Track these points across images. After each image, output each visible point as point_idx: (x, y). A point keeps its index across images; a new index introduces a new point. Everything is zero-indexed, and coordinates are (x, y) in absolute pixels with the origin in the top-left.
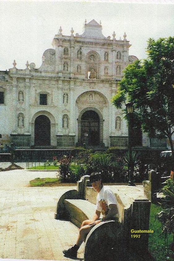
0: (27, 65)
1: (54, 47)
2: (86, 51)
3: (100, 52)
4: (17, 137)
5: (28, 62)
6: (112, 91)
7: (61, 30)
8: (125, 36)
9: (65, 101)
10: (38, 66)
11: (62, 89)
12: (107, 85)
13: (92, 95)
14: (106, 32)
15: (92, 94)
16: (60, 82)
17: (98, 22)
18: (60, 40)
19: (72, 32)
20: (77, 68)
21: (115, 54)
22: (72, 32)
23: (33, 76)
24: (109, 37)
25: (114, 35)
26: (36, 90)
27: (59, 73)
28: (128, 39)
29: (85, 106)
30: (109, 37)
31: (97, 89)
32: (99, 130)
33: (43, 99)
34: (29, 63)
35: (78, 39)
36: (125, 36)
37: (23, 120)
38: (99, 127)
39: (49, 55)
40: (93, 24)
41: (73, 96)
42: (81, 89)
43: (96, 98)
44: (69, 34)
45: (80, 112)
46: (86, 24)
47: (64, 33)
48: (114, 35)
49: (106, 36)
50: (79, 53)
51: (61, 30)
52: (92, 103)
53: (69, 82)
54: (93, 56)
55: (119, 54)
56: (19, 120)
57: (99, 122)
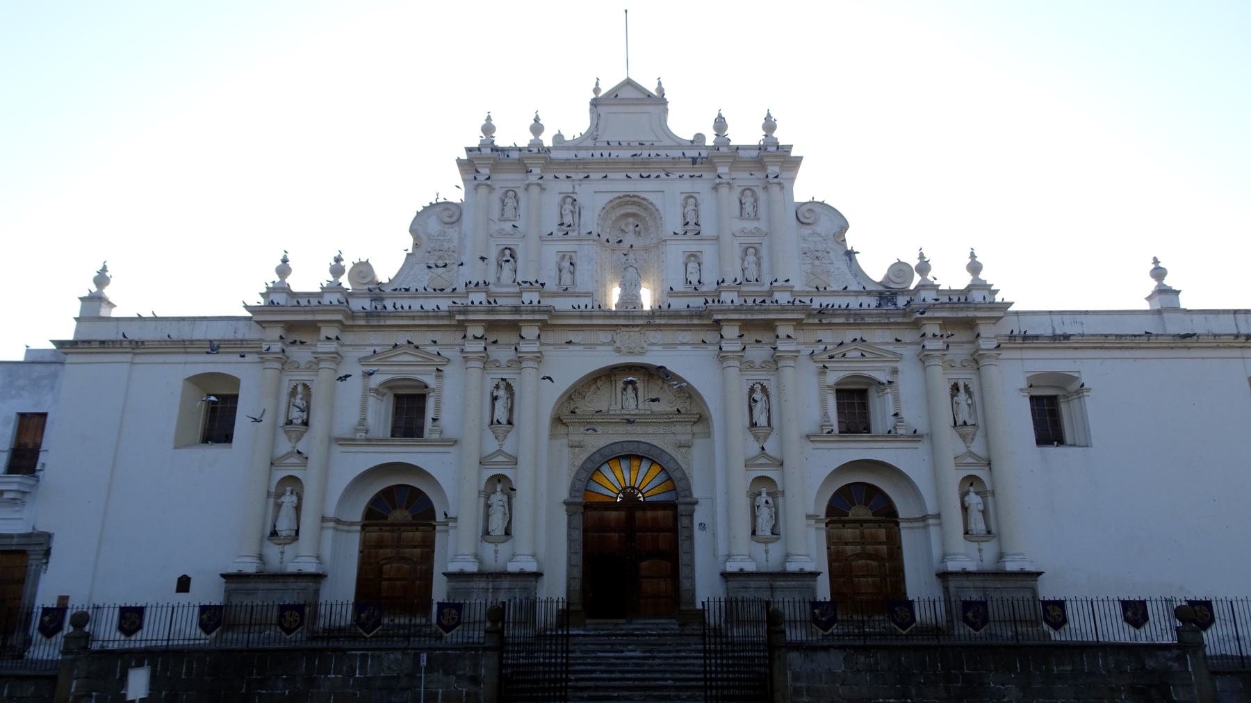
0: (337, 270)
1: (453, 190)
3: (667, 197)
4: (251, 585)
6: (722, 357)
7: (488, 129)
8: (769, 125)
10: (385, 271)
13: (635, 389)
14: (688, 121)
17: (652, 89)
18: (484, 163)
19: (537, 128)
20: (560, 271)
21: (730, 199)
22: (537, 128)
23: (353, 315)
24: (700, 137)
30: (700, 137)
31: (654, 358)
33: (410, 411)
34: (348, 265)
36: (769, 125)
37: (298, 508)
38: (674, 530)
39: (434, 224)
40: (628, 93)
44: (523, 139)
45: (579, 462)
46: (594, 100)
47: (502, 140)
49: (687, 135)
51: (488, 129)
55: (748, 201)
56: (278, 506)
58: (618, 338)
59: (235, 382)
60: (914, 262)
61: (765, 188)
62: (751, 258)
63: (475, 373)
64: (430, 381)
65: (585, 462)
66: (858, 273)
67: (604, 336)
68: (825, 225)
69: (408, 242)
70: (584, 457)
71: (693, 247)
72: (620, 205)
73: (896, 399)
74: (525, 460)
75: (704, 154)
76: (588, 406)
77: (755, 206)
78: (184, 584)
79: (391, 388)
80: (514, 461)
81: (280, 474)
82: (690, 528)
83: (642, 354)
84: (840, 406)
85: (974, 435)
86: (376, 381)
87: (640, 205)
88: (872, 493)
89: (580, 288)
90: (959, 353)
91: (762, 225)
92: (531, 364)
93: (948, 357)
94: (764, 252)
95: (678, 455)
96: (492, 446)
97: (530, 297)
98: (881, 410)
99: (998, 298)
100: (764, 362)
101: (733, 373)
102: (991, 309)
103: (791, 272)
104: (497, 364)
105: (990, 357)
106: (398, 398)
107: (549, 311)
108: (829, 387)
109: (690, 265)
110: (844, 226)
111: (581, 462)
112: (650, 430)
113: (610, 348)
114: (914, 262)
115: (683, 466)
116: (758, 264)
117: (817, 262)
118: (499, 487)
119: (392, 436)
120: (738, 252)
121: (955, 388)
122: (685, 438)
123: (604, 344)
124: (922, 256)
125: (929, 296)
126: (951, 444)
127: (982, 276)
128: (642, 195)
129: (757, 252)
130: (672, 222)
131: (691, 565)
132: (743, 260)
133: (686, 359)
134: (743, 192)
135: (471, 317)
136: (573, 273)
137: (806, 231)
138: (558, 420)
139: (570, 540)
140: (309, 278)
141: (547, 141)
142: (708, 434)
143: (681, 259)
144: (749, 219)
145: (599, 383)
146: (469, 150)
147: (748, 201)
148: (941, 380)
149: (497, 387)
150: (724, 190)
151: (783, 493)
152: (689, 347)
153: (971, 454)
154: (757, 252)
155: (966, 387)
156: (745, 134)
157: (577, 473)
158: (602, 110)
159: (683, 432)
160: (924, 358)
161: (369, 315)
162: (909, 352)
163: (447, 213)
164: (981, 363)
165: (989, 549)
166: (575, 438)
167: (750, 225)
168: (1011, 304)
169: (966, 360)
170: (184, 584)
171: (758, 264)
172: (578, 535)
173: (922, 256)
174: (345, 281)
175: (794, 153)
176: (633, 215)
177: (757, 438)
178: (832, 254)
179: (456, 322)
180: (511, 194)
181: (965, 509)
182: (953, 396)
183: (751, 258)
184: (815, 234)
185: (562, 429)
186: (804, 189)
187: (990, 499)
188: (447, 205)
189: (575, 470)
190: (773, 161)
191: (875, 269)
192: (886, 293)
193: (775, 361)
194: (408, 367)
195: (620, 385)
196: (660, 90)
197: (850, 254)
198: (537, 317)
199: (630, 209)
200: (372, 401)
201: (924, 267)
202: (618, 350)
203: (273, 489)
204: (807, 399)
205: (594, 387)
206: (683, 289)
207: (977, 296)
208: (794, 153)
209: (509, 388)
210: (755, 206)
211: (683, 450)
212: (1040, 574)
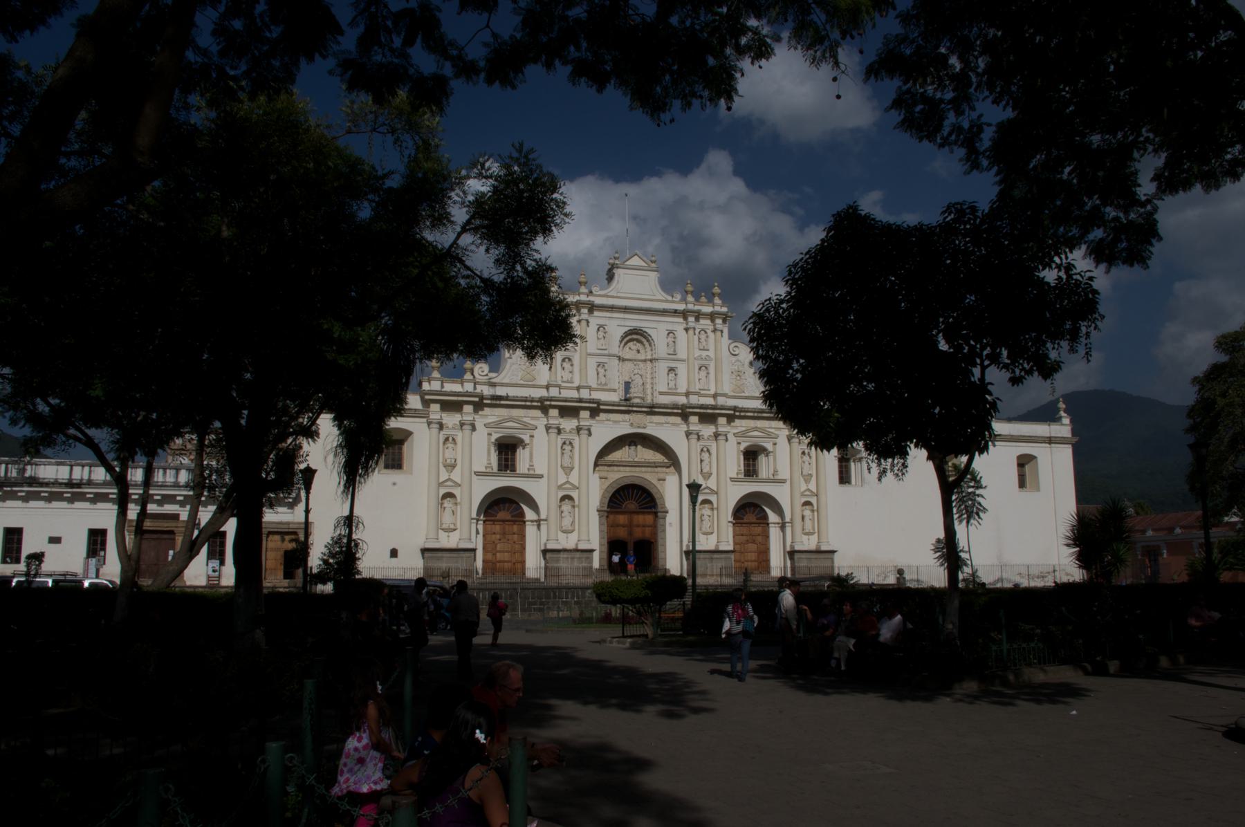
3: (657, 328)
4: (440, 554)
12: (678, 420)
23: (482, 397)
26: (490, 434)
29: (617, 476)
31: (651, 430)
32: (655, 534)
38: (654, 526)
42: (607, 429)
45: (605, 487)
50: (601, 334)
55: (703, 336)
57: (656, 514)
59: (408, 434)
64: (526, 438)
70: (608, 483)
71: (673, 365)
73: (775, 460)
76: (617, 456)
78: (394, 553)
81: (443, 491)
82: (664, 525)
88: (756, 506)
96: (562, 479)
122: (661, 476)
130: (661, 348)
131: (664, 545)
133: (670, 432)
137: (734, 359)
138: (596, 465)
139: (601, 531)
150: (691, 332)
165: (814, 539)
166: (604, 474)
167: (704, 353)
170: (394, 553)
172: (605, 528)
179: (543, 406)
181: (803, 517)
194: (510, 429)
202: (632, 425)
212: (833, 552)
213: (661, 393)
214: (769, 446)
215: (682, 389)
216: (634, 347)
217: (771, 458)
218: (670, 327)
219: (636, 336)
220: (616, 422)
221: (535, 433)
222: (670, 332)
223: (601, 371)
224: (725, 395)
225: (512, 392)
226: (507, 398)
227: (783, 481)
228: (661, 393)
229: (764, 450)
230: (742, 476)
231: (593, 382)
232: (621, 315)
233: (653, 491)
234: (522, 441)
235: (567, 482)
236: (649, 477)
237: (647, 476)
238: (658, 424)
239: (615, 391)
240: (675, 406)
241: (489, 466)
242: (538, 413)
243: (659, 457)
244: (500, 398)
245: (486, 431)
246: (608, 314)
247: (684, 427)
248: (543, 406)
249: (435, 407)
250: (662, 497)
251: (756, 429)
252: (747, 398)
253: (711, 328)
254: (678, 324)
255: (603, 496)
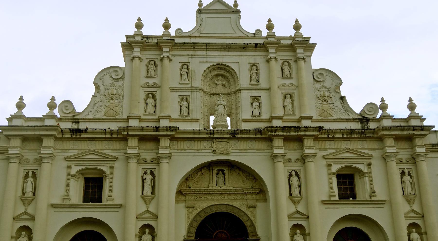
0: (52, 106)
1: (118, 60)
2: (200, 64)
3: (241, 64)
5: (53, 99)
6: (274, 157)
7: (139, 25)
8: (297, 27)
9: (148, 190)
10: (80, 107)
11: (140, 161)
15: (223, 171)
16: (133, 142)
19: (167, 26)
20: (181, 107)
21: (276, 67)
22: (167, 26)
23: (62, 131)
25: (270, 26)
27: (130, 121)
28: (305, 32)
31: (235, 156)
33: (94, 188)
34: (58, 102)
35: (177, 41)
36: (297, 27)
39: (107, 79)
41: (172, 175)
43: (233, 182)
44: (159, 31)
45: (192, 217)
48: (270, 26)
49: (251, 30)
50: (185, 70)
52: (225, 195)
53: (156, 140)
54: (222, 75)
55: (286, 68)
58: (214, 145)
60: (378, 103)
61: (296, 61)
62: (288, 100)
63: (133, 166)
64: (106, 170)
65: (195, 217)
66: (348, 109)
67: (206, 144)
68: (329, 80)
69: (92, 91)
70: (194, 213)
71: (256, 94)
72: (214, 70)
73: (371, 181)
74: (163, 216)
75: (261, 41)
77: (290, 72)
79: (82, 174)
80: (156, 217)
83: (227, 154)
84: (339, 184)
85: (414, 200)
86: (74, 170)
87: (225, 70)
89: (193, 116)
90: (404, 154)
91: (294, 82)
92: (165, 160)
93: (399, 157)
94: (295, 97)
95: (248, 212)
97: (164, 123)
98: (362, 188)
99: (425, 123)
100: (297, 159)
101: (280, 165)
102: (422, 130)
103: (310, 109)
104: (145, 161)
105: (422, 156)
106: (87, 180)
107: (175, 129)
108: (333, 173)
109: (254, 104)
110: (341, 83)
111: (193, 216)
112: (233, 197)
113: (210, 151)
114: (378, 103)
115: (252, 218)
116: (292, 104)
117: (325, 103)
118: (147, 230)
119: (84, 201)
120: (281, 97)
121: (403, 173)
122: (251, 203)
123: (206, 149)
124: (383, 100)
125: (387, 123)
126: (403, 207)
127: (416, 111)
128: (227, 64)
129: (291, 97)
130: (244, 80)
132: (284, 101)
134: (283, 64)
135: (130, 133)
136: (188, 108)
137: (318, 86)
138: (180, 193)
140: (35, 110)
141: (173, 34)
142: (265, 200)
143: (250, 100)
144: (287, 78)
145: (203, 171)
146: (127, 37)
147: (286, 68)
148: (395, 169)
149: (146, 173)
150: (273, 62)
151: (309, 234)
152: (255, 151)
153: (413, 211)
154: (291, 97)
155: (409, 174)
156: (283, 30)
157: (191, 223)
158: (203, 16)
159: (251, 199)
160: (385, 158)
161: (72, 131)
162: (376, 154)
163: (116, 73)
164: (417, 160)
166: (190, 203)
167: (288, 82)
168: (433, 127)
169: (408, 159)
171: (292, 104)
173: (383, 100)
174: (56, 112)
175: (311, 42)
176: (222, 75)
177: (294, 202)
178: (333, 98)
179: (121, 136)
180: (152, 62)
182: (402, 178)
183: (288, 100)
184: (323, 87)
185: (183, 198)
186: (318, 61)
187: (424, 236)
188: (115, 69)
189: (190, 221)
190: (300, 46)
191: (357, 106)
192: (364, 119)
193: (303, 160)
194: (92, 162)
195: (215, 171)
196: (236, 5)
197: (343, 98)
198: (169, 133)
199: (219, 72)
200: (72, 182)
201: (384, 107)
202: (214, 152)
203: (14, 234)
204: (321, 182)
205: (200, 173)
206: (251, 118)
207: (414, 123)
208: (311, 42)
209: (152, 173)
210: (290, 72)
211: (252, 209)
213: (245, 121)
214: (363, 168)
215: (265, 116)
216: (220, 82)
217: (367, 179)
218: (252, 60)
219: (222, 73)
220: (197, 150)
221: (116, 165)
222: (253, 65)
223: (184, 103)
224: (310, 118)
225: (91, 126)
226: (86, 131)
227: (381, 203)
228: (245, 121)
229: (359, 171)
230: (337, 198)
231: (175, 115)
232: (204, 53)
233: (244, 219)
234: (104, 172)
235: (148, 211)
236: (239, 204)
237: (236, 204)
238: (241, 150)
239: (197, 120)
240: (258, 131)
241: (66, 197)
242: (117, 145)
243: (247, 185)
244: (79, 131)
245: (66, 164)
246: (191, 53)
247: (267, 153)
248: (121, 136)
249: (17, 142)
250: (253, 225)
251: (348, 151)
252: (335, 121)
253: (293, 59)
254: (258, 57)
255: (191, 226)
